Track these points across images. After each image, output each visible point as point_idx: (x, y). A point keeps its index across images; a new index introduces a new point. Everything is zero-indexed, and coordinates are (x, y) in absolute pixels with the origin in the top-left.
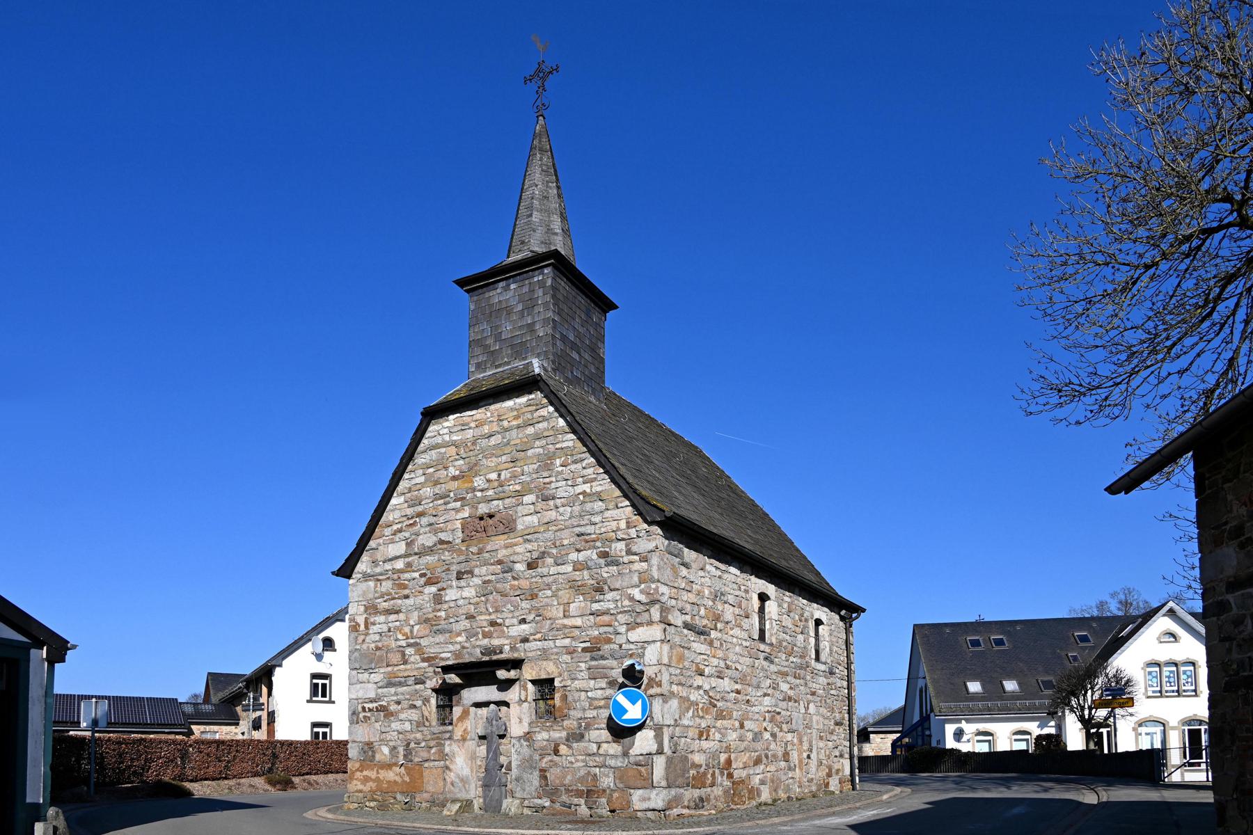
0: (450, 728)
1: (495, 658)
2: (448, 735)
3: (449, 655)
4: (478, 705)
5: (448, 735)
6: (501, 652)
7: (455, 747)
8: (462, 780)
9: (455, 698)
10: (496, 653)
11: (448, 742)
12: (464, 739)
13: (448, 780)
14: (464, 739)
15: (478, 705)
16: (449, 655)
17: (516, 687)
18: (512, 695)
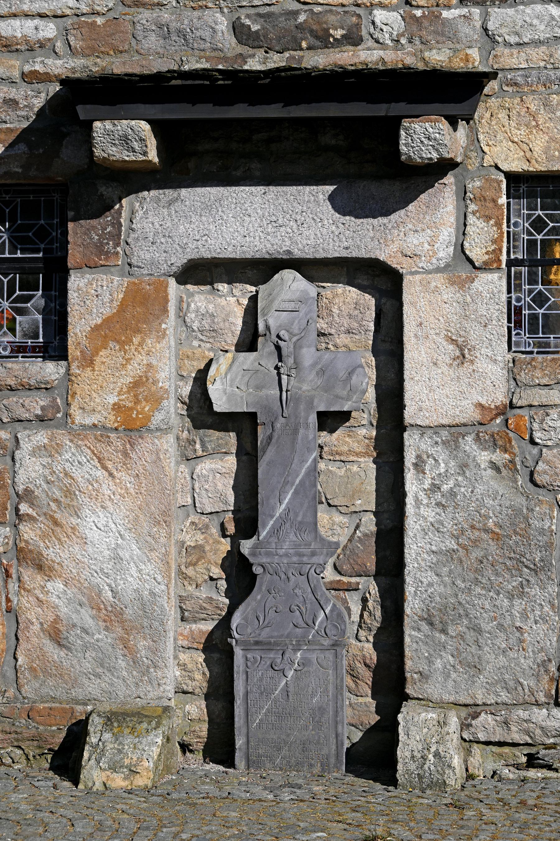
0: (52, 370)
1: (320, 60)
2: (36, 404)
3: (49, 30)
4: (201, 272)
5: (36, 404)
6: (353, 39)
7: (78, 463)
8: (113, 616)
9: (80, 235)
10: (323, 40)
11: (33, 439)
12: (131, 426)
13: (31, 613)
14: (131, 426)
15: (201, 272)
16: (49, 30)
17: (442, 201)
18: (418, 235)
